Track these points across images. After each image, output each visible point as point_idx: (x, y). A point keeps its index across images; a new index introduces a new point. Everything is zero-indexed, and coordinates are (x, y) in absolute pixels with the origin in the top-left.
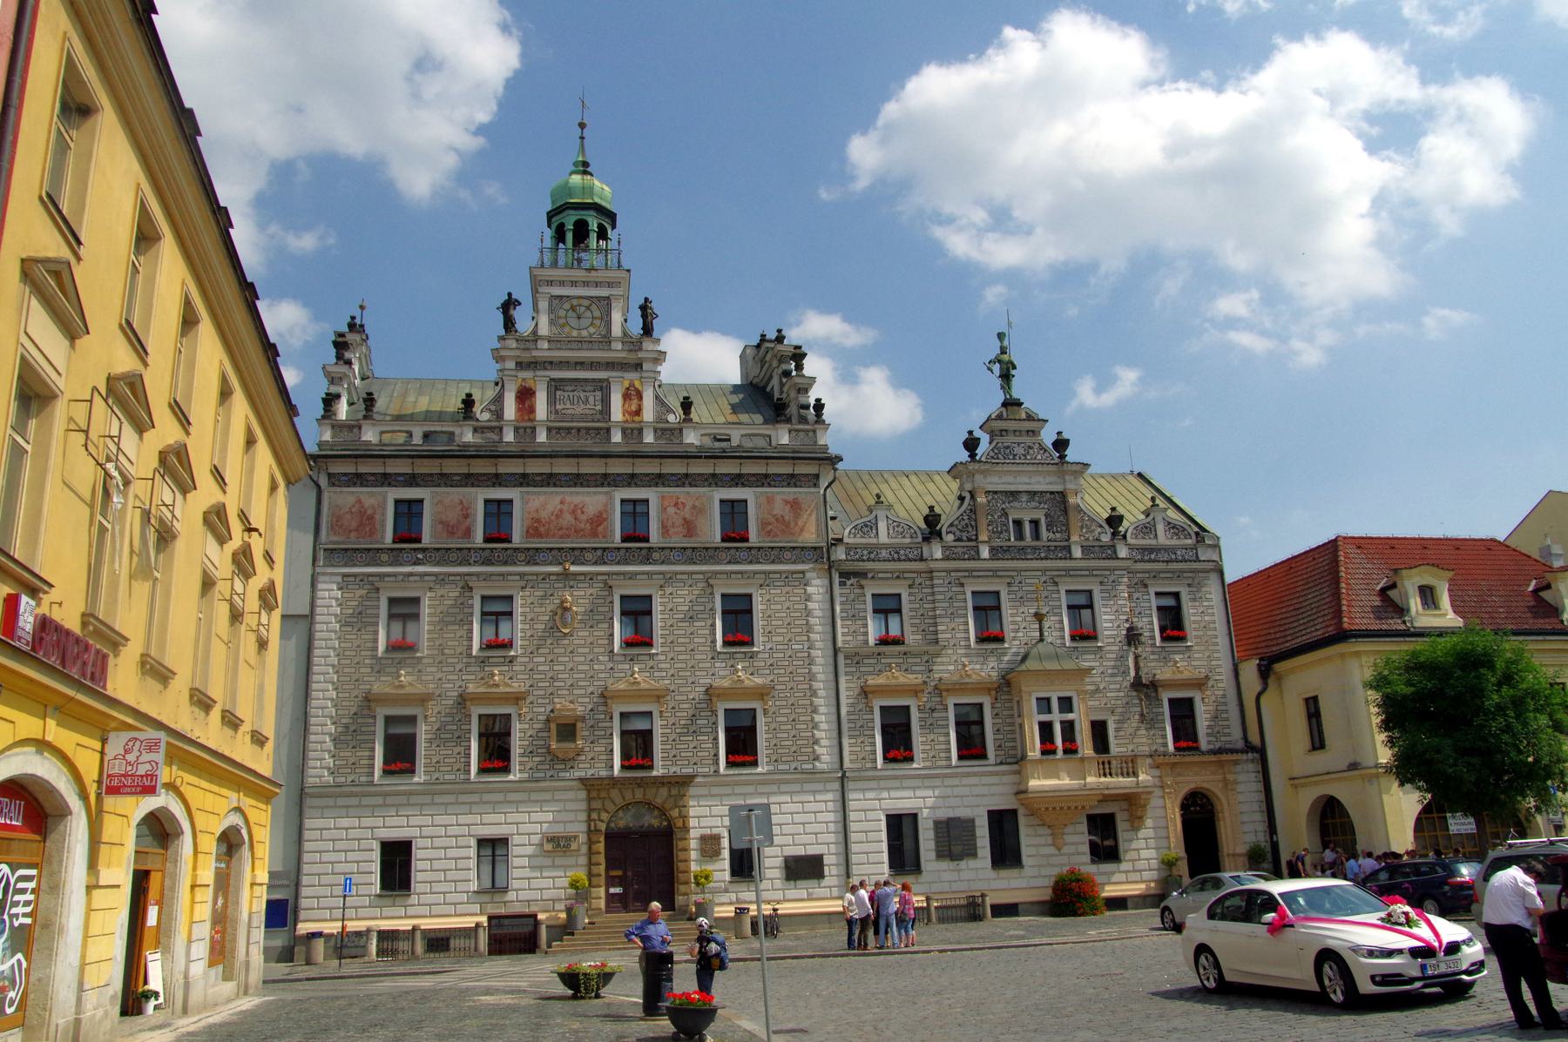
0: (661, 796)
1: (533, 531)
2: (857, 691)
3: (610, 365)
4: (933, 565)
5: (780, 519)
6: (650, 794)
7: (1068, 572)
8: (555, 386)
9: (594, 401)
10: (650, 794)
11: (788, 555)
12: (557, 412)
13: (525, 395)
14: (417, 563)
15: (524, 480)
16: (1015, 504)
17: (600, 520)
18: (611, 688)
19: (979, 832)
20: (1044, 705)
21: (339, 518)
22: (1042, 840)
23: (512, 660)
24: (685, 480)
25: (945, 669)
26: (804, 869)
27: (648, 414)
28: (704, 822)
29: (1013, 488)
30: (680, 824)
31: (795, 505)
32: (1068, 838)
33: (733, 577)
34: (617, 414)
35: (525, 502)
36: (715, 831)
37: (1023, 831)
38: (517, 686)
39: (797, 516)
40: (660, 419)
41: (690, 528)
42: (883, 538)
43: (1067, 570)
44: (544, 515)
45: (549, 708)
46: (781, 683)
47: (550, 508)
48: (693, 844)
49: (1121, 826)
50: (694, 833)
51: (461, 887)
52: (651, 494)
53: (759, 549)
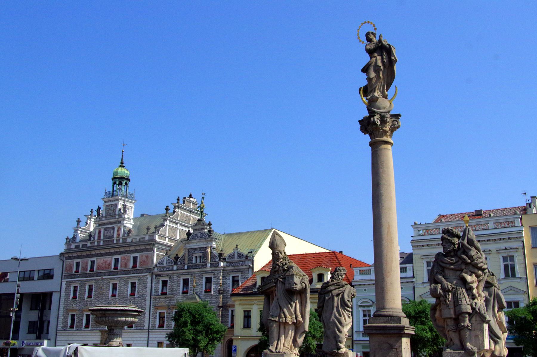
1: (98, 269)
3: (115, 223)
5: (144, 261)
7: (206, 272)
8: (106, 229)
11: (144, 271)
14: (79, 277)
15: (97, 255)
17: (110, 264)
23: (92, 301)
27: (122, 235)
29: (195, 247)
34: (115, 236)
35: (97, 261)
41: (126, 265)
42: (165, 265)
52: (119, 257)
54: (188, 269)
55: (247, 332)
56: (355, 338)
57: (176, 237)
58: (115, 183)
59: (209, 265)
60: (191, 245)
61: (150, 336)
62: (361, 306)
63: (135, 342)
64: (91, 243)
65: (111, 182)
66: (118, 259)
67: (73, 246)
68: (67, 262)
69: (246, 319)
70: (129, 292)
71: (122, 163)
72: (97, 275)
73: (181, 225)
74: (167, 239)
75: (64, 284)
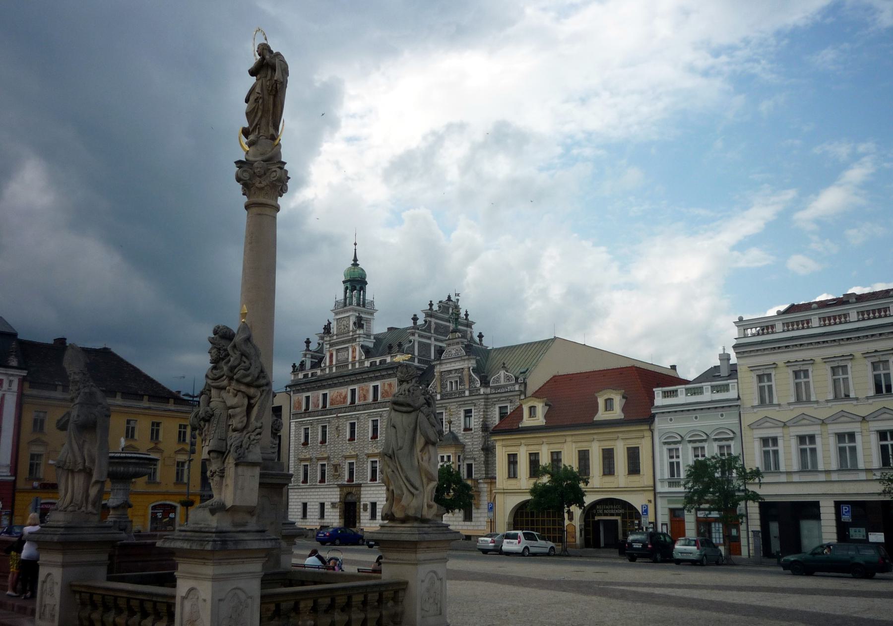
1: (331, 404)
13: (331, 356)
15: (330, 386)
17: (345, 397)
24: (365, 380)
27: (357, 359)
31: (390, 385)
34: (350, 360)
38: (325, 456)
40: (360, 359)
41: (365, 398)
55: (512, 484)
56: (659, 489)
57: (430, 356)
58: (346, 288)
59: (467, 393)
60: (444, 366)
62: (665, 443)
64: (322, 370)
65: (342, 287)
67: (301, 376)
68: (295, 397)
69: (512, 466)
70: (370, 435)
71: (355, 260)
72: (330, 412)
73: (436, 340)
74: (416, 360)
75: (293, 425)
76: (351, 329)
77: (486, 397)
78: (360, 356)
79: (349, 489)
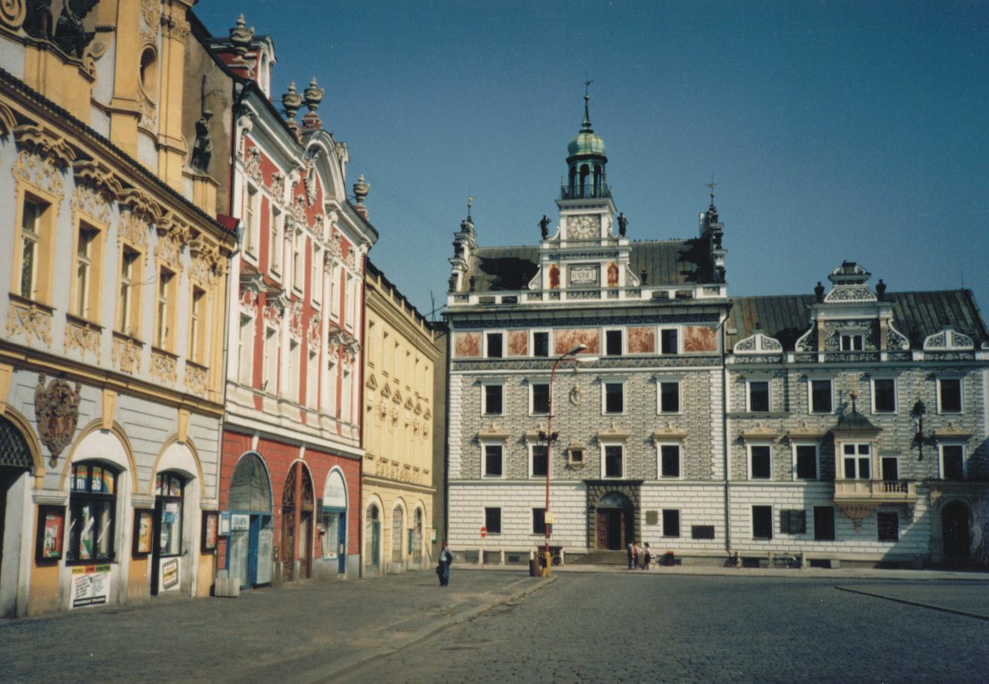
0: (626, 490)
1: (560, 348)
2: (737, 437)
3: (600, 254)
4: (787, 366)
6: (620, 489)
8: (571, 267)
9: (592, 275)
10: (620, 489)
12: (571, 283)
13: (555, 274)
16: (846, 328)
18: (600, 434)
19: (807, 519)
20: (849, 449)
21: (460, 345)
22: (848, 526)
25: (792, 425)
26: (703, 532)
28: (649, 505)
30: (635, 504)
32: (864, 526)
33: (667, 371)
34: (604, 283)
36: (655, 510)
37: (837, 521)
39: (706, 338)
42: (759, 350)
43: (877, 368)
44: (565, 340)
45: (568, 443)
46: (693, 432)
47: (568, 337)
48: (643, 517)
49: (900, 521)
50: (643, 511)
51: (525, 532)
53: (683, 358)
54: (797, 362)
59: (884, 357)
61: (731, 494)
63: (687, 505)
66: (619, 334)
76: (604, 235)
77: (920, 366)
78: (628, 281)
79: (614, 488)
